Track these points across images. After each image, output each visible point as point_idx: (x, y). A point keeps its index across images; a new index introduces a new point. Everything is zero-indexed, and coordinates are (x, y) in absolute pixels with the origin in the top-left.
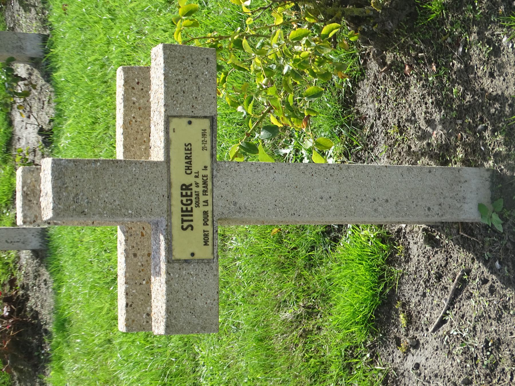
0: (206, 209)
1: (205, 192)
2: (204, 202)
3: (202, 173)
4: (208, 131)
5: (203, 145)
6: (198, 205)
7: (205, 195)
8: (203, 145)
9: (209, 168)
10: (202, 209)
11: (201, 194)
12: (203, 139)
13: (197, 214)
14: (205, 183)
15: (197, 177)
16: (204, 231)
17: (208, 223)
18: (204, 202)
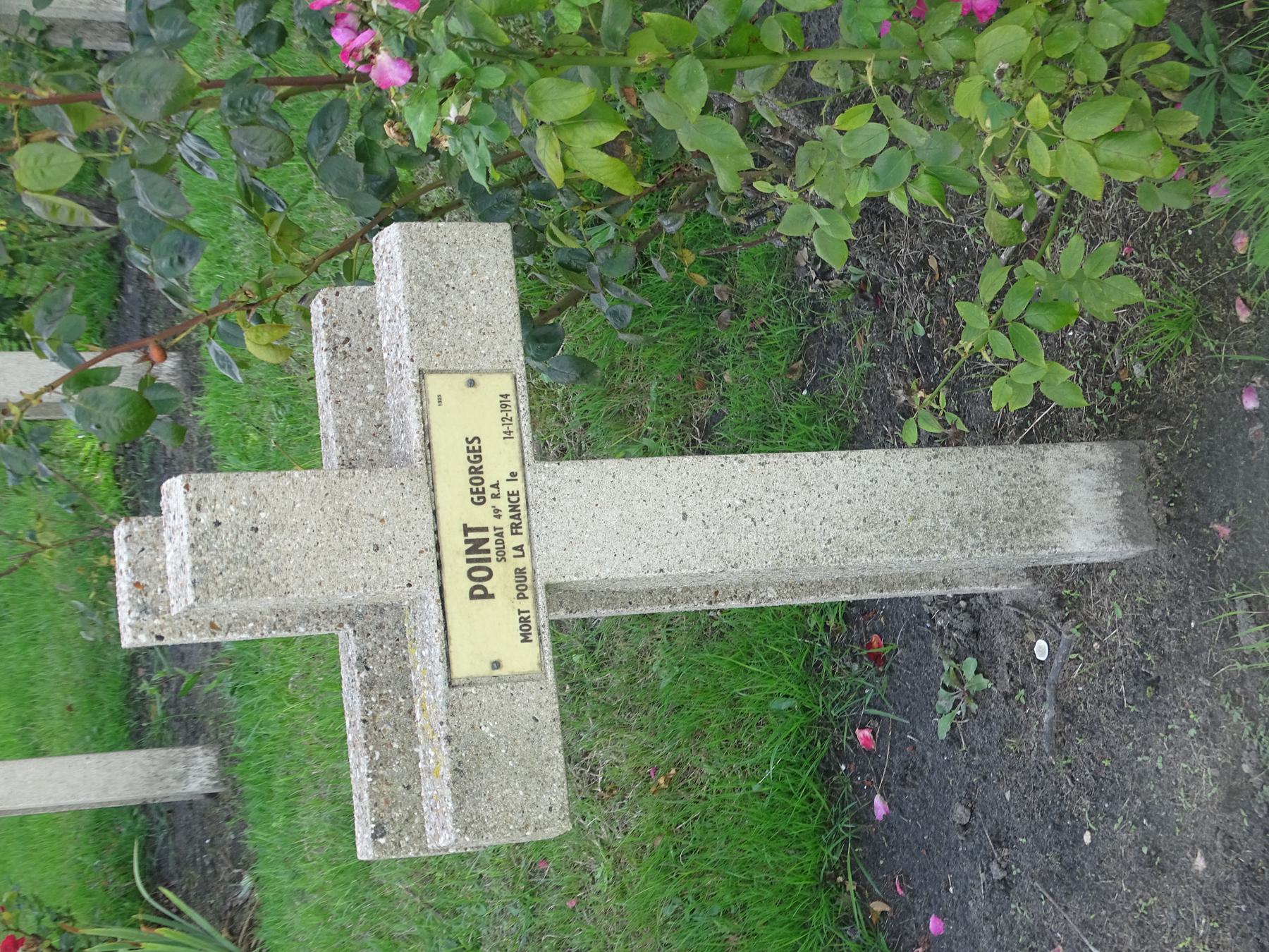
0: (521, 563)
1: (515, 529)
2: (515, 548)
3: (506, 487)
4: (512, 398)
5: (505, 428)
6: (502, 558)
7: (517, 533)
8: (505, 428)
9: (520, 477)
10: (513, 563)
11: (507, 531)
12: (504, 414)
13: (502, 580)
14: (514, 508)
15: (495, 496)
16: (520, 612)
17: (527, 593)
18: (515, 548)
